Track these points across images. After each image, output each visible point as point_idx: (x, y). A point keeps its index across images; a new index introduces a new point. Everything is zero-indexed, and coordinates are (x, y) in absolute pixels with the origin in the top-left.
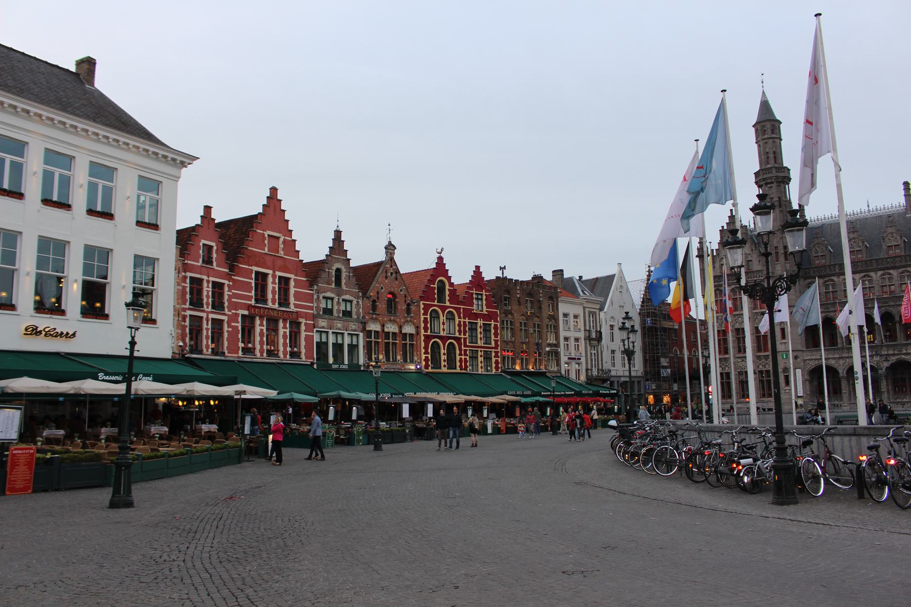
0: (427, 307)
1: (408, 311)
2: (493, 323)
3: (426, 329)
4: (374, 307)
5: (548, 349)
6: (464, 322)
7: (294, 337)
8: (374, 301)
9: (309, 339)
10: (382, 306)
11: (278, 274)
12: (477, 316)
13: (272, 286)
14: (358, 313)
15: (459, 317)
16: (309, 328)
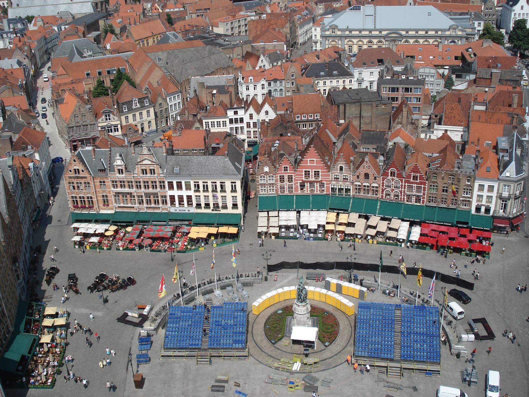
0: (383, 179)
1: (375, 178)
2: (423, 186)
3: (383, 186)
4: (358, 177)
5: (461, 199)
6: (405, 186)
7: (322, 185)
8: (358, 176)
9: (328, 188)
10: (362, 177)
11: (313, 170)
12: (412, 183)
13: (312, 174)
14: (350, 180)
15: (402, 183)
16: (327, 184)
